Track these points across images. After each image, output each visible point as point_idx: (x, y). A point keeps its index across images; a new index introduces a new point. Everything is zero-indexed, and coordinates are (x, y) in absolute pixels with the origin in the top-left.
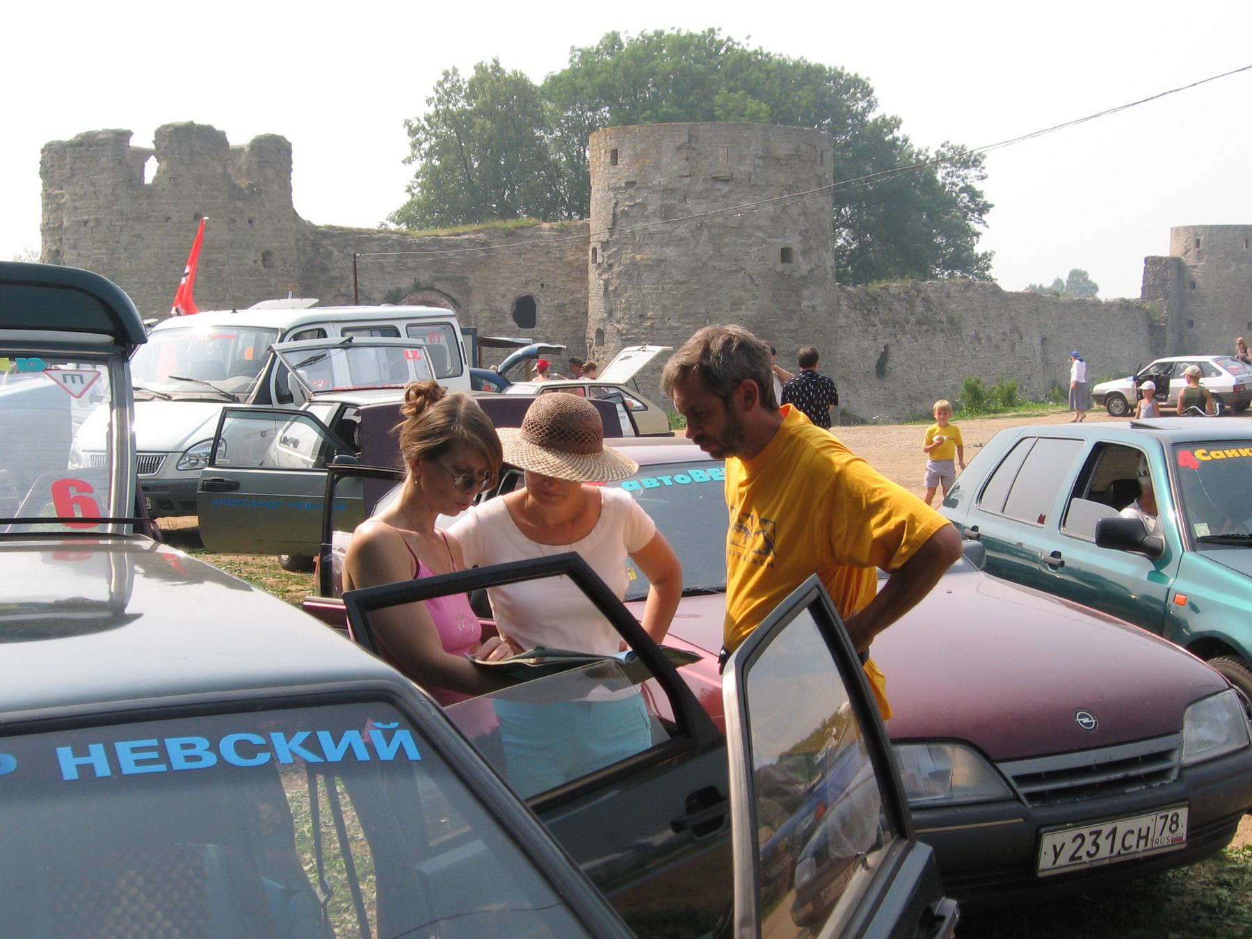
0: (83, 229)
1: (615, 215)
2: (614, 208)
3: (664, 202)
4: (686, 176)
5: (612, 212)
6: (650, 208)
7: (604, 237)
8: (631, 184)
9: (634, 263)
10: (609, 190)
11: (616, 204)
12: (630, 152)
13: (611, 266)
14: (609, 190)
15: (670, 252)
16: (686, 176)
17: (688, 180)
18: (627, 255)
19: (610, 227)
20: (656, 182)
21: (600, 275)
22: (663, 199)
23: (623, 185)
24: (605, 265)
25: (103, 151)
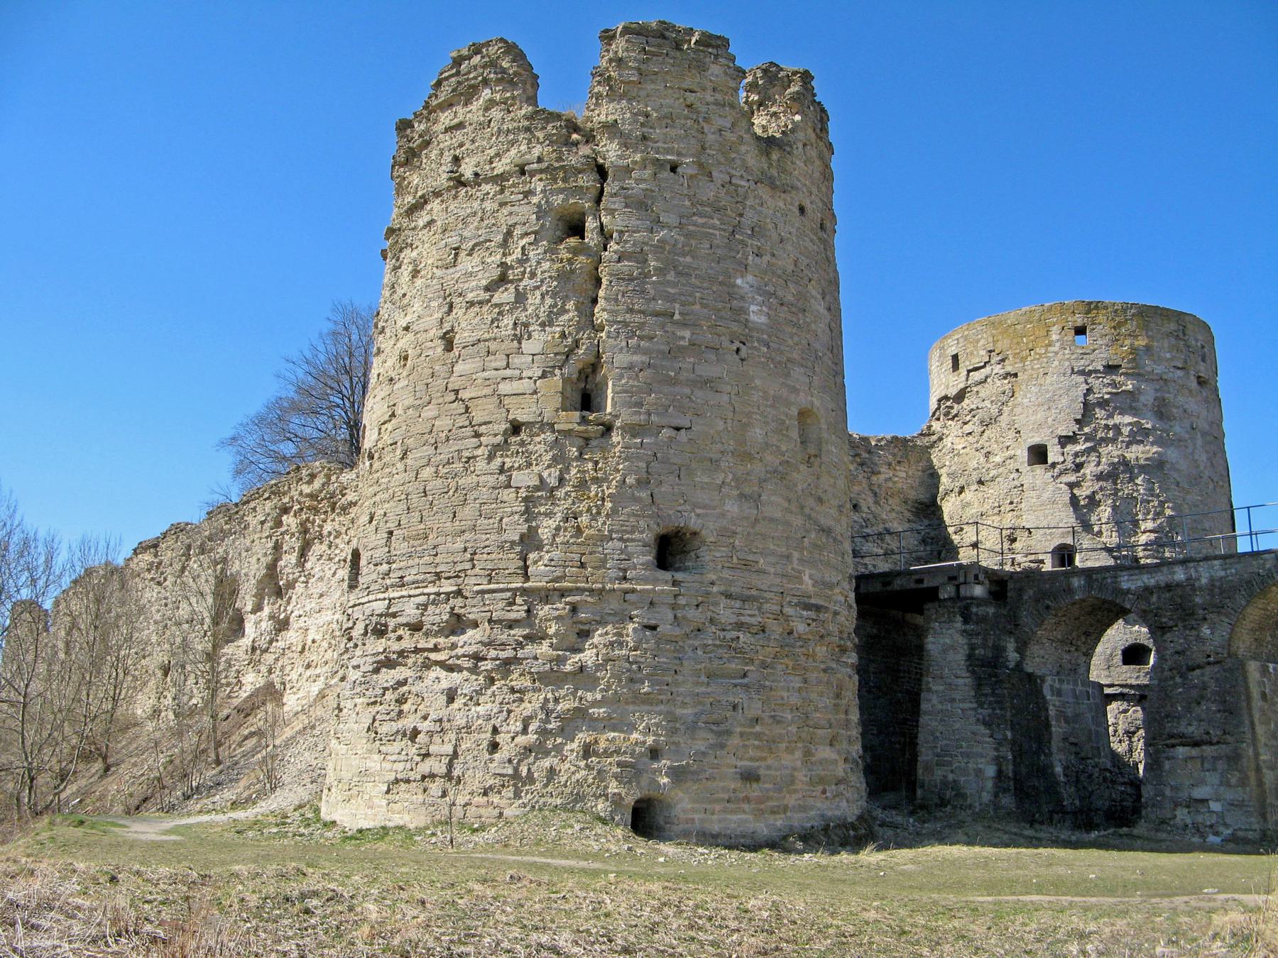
0: (666, 174)
1: (1085, 404)
2: (1086, 395)
3: (1158, 394)
4: (1179, 368)
5: (1081, 399)
6: (1142, 399)
7: (1067, 429)
8: (1111, 369)
9: (1125, 462)
10: (1073, 372)
11: (1089, 391)
12: (1107, 330)
13: (1079, 467)
14: (1073, 372)
15: (1172, 454)
16: (1179, 368)
17: (1179, 373)
18: (1111, 453)
19: (1079, 417)
20: (1148, 369)
21: (1055, 478)
22: (1156, 390)
23: (1101, 368)
24: (1069, 465)
25: (716, 56)
